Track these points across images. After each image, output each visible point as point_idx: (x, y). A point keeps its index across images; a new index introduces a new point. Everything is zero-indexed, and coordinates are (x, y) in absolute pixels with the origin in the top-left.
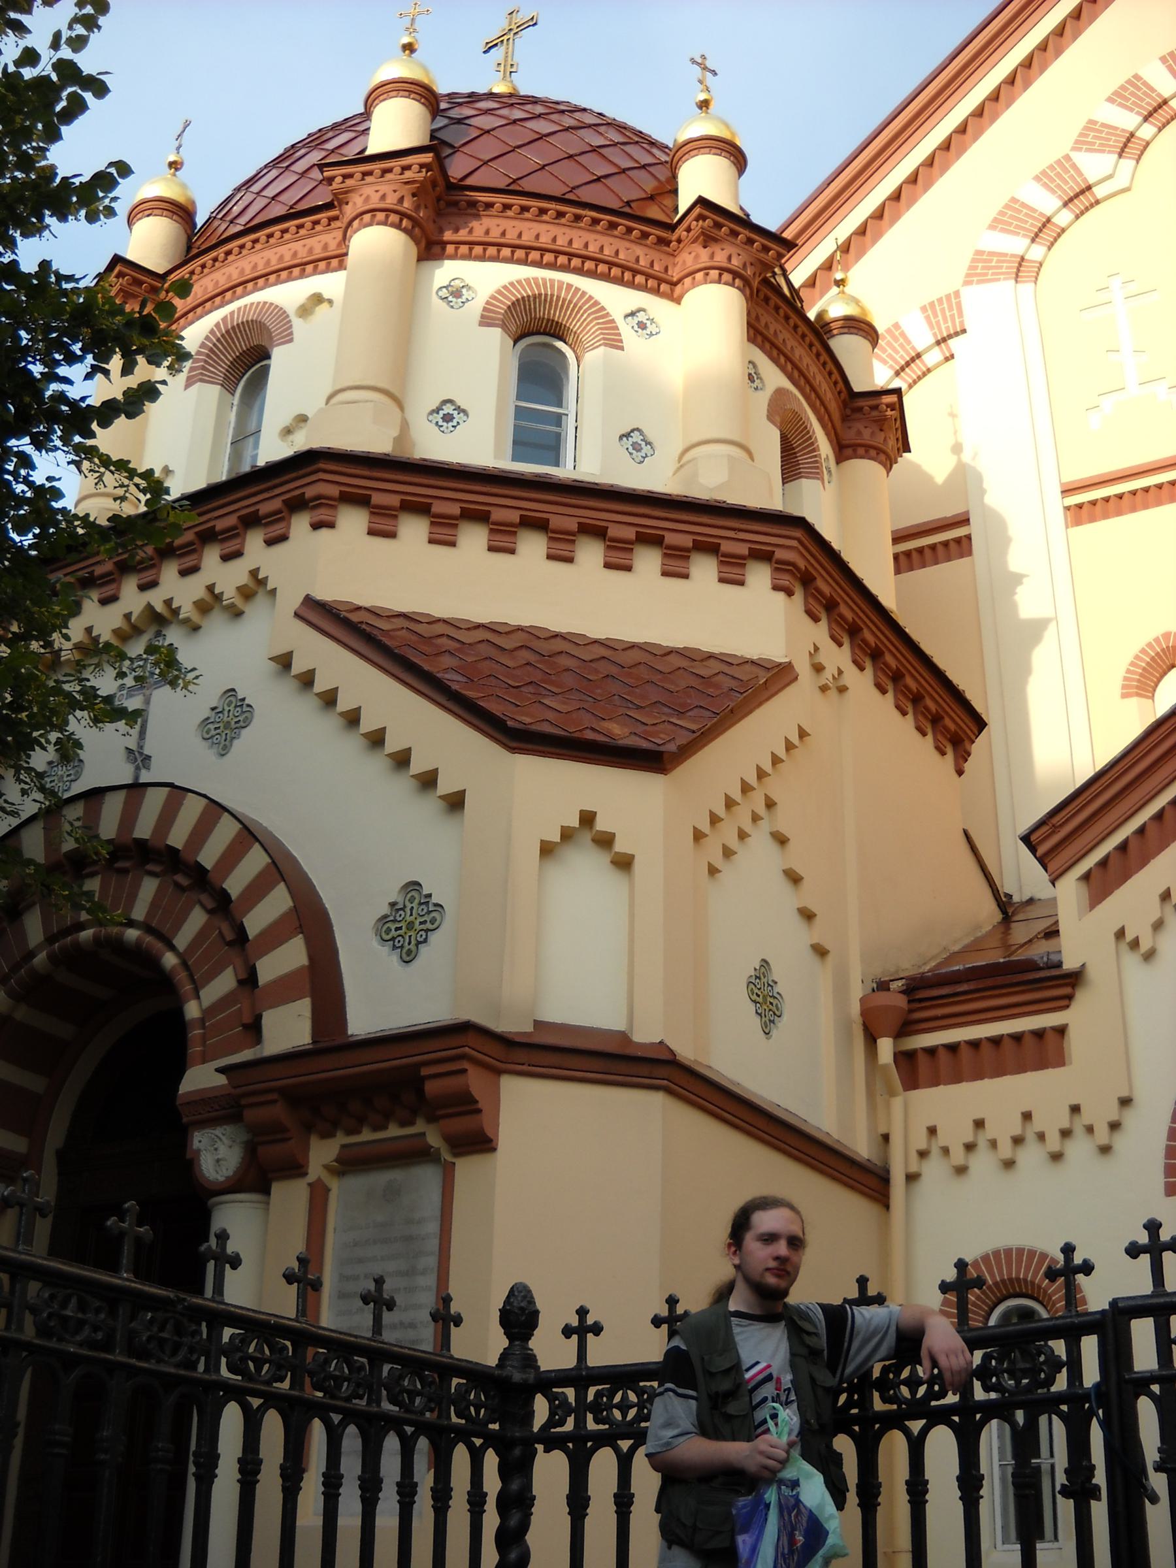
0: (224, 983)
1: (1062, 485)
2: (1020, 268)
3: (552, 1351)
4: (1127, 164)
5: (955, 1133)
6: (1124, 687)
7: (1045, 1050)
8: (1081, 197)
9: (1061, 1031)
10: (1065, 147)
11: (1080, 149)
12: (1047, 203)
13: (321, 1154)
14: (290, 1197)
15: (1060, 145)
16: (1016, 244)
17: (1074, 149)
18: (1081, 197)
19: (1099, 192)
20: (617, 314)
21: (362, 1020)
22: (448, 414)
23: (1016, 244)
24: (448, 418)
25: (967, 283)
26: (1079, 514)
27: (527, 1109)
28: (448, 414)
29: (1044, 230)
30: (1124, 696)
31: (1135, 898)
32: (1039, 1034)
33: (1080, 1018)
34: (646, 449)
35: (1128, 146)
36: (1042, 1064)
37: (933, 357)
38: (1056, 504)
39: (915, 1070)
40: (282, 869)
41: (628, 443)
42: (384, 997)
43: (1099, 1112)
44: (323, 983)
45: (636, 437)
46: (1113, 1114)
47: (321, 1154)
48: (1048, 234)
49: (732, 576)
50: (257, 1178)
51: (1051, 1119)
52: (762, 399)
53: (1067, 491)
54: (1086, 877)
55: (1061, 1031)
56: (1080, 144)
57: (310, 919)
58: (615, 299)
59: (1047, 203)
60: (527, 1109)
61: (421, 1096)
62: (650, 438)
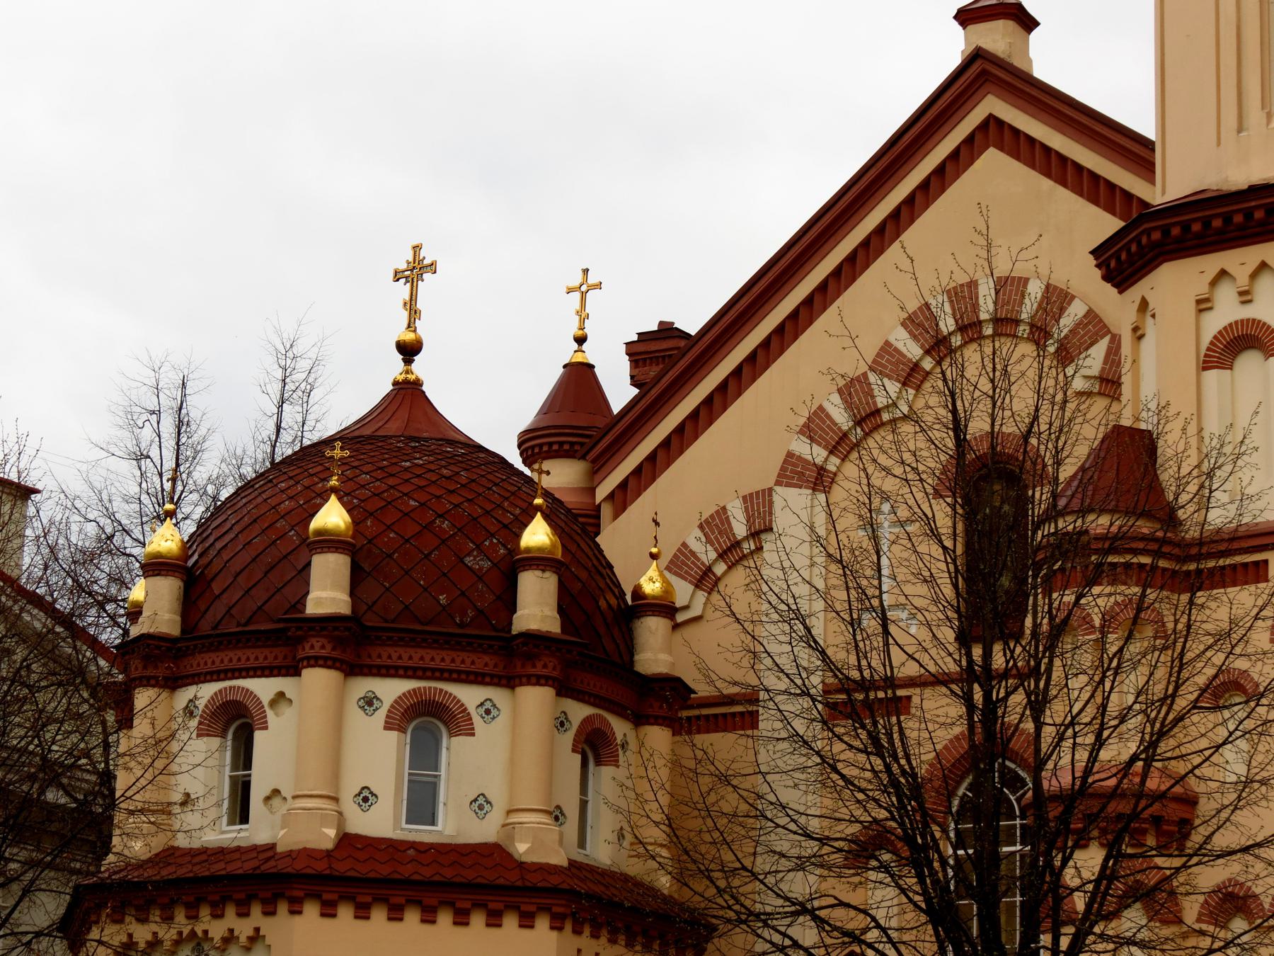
8: (869, 419)
10: (864, 367)
17: (871, 369)
18: (869, 419)
20: (472, 709)
22: (366, 798)
24: (366, 800)
25: (778, 483)
28: (366, 798)
34: (487, 807)
37: (748, 546)
41: (475, 806)
45: (481, 801)
48: (843, 449)
49: (527, 921)
52: (568, 738)
58: (469, 696)
62: (490, 799)
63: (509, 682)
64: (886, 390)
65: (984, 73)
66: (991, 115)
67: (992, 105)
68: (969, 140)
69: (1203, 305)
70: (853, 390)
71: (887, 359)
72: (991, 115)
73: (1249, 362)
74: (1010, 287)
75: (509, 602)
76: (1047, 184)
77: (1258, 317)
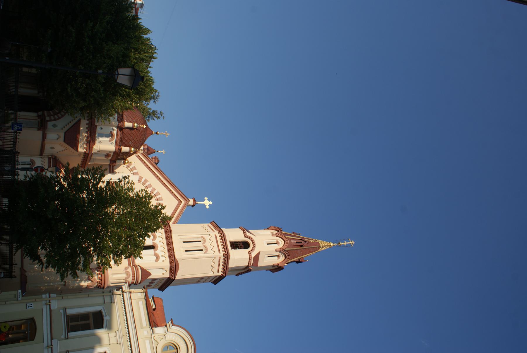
0: (52, 114)
3: (18, 134)
5: (44, 161)
13: (39, 120)
14: (37, 118)
15: (153, 186)
21: (49, 123)
27: (40, 133)
39: (49, 158)
40: (59, 118)
42: (50, 124)
44: (51, 120)
47: (39, 120)
50: (39, 116)
56: (153, 188)
57: (55, 120)
58: (114, 141)
60: (40, 133)
61: (42, 126)
63: (116, 145)
75: (126, 146)
76: (174, 209)
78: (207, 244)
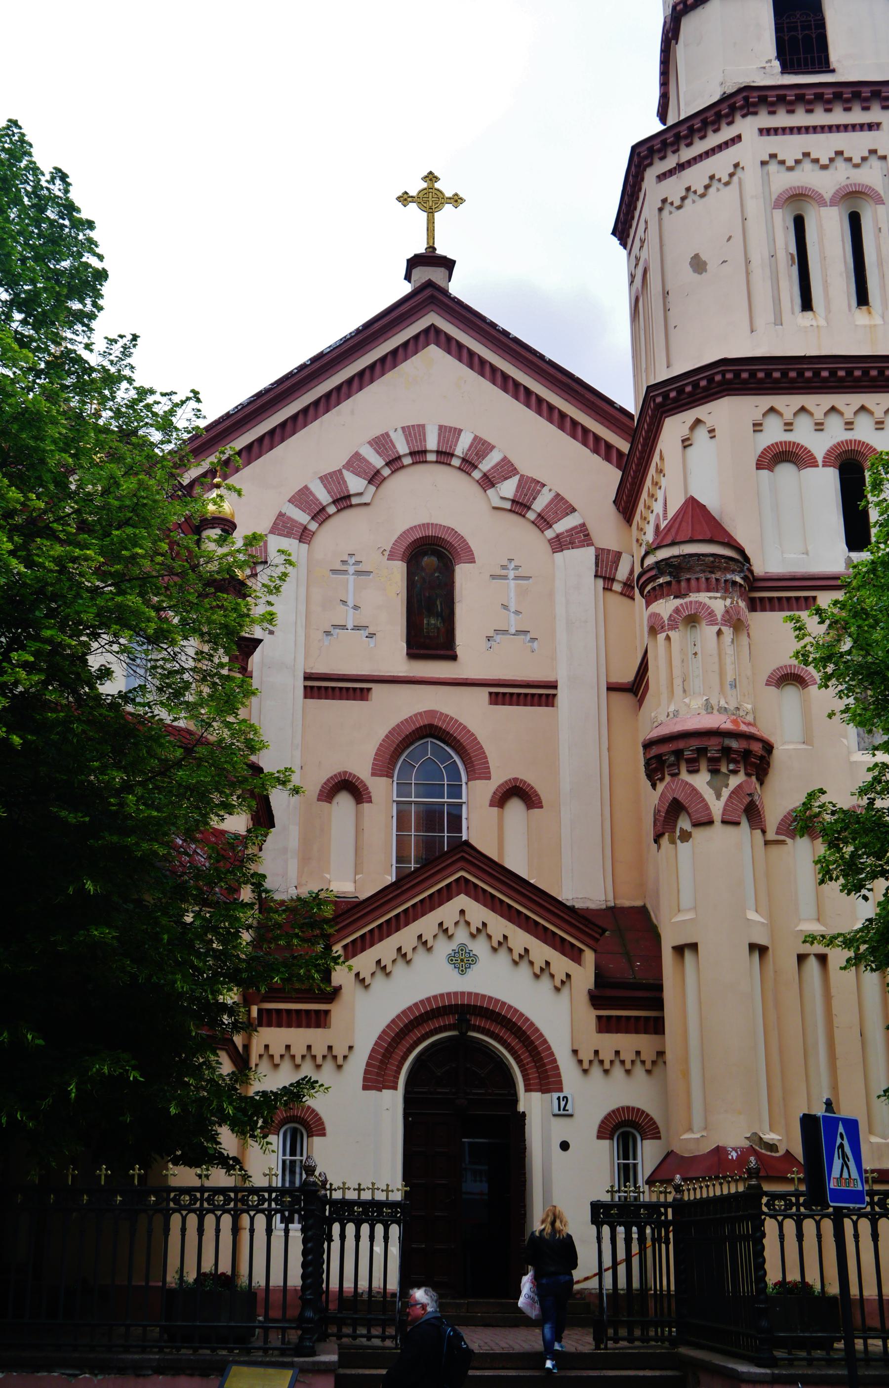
1: (305, 673)
2: (304, 535)
4: (372, 488)
6: (319, 795)
7: (320, 1020)
8: (344, 501)
9: (327, 1012)
10: (340, 466)
11: (348, 470)
12: (323, 496)
16: (302, 517)
18: (344, 501)
19: (354, 501)
23: (302, 517)
25: (271, 532)
26: (311, 692)
29: (320, 515)
30: (319, 800)
31: (364, 962)
32: (317, 1012)
33: (337, 1011)
35: (375, 478)
36: (318, 1026)
38: (300, 684)
43: (340, 1051)
46: (346, 1053)
48: (321, 518)
51: (319, 1050)
53: (308, 677)
54: (345, 947)
55: (327, 1012)
56: (349, 465)
59: (323, 496)
64: (355, 483)
65: (432, 297)
66: (433, 324)
67: (432, 318)
68: (416, 337)
69: (757, 427)
70: (332, 479)
71: (356, 463)
72: (433, 324)
73: (786, 470)
74: (449, 433)
77: (797, 441)
78: (827, 183)
